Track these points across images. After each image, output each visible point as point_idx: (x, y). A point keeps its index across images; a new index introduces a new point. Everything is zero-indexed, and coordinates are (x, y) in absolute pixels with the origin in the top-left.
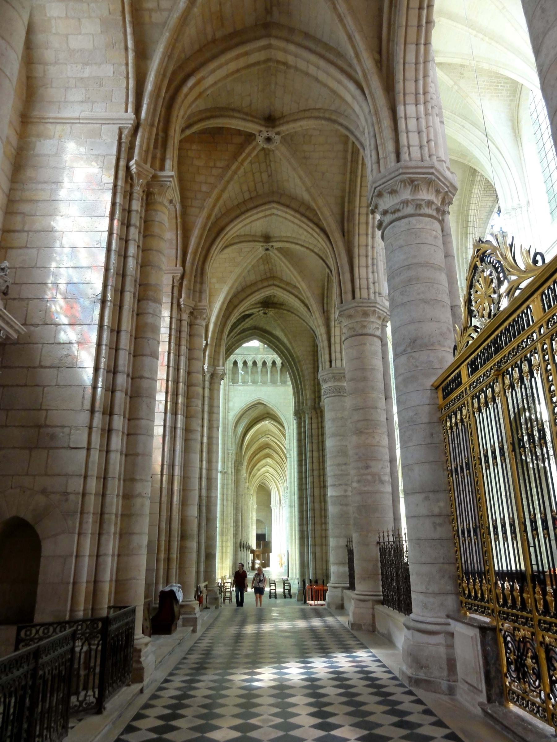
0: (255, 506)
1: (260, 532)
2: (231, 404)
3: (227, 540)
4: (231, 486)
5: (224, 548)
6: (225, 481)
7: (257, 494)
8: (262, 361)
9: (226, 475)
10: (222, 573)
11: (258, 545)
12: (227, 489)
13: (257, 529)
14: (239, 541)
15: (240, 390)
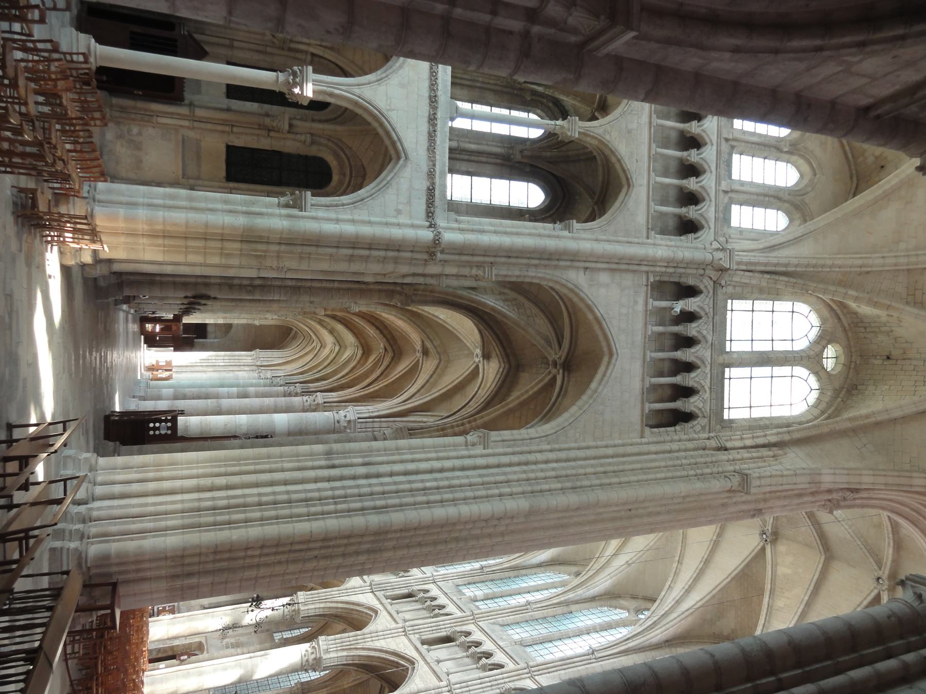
0: (257, 323)
1: (209, 329)
2: (604, 277)
3: (229, 255)
4: (371, 271)
5: (201, 244)
6: (408, 255)
7: (276, 326)
8: (699, 362)
9: (426, 257)
10: (115, 233)
11: (188, 327)
12: (384, 260)
13: (216, 325)
14: (212, 294)
15: (636, 302)
